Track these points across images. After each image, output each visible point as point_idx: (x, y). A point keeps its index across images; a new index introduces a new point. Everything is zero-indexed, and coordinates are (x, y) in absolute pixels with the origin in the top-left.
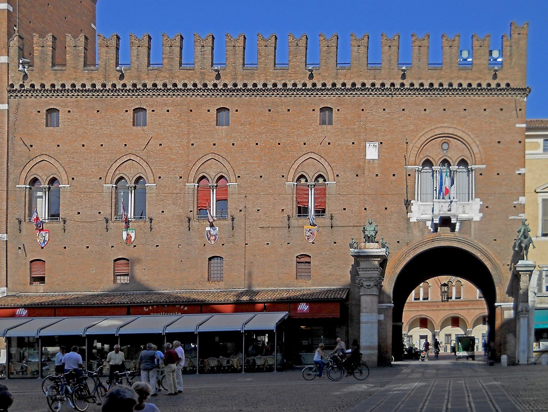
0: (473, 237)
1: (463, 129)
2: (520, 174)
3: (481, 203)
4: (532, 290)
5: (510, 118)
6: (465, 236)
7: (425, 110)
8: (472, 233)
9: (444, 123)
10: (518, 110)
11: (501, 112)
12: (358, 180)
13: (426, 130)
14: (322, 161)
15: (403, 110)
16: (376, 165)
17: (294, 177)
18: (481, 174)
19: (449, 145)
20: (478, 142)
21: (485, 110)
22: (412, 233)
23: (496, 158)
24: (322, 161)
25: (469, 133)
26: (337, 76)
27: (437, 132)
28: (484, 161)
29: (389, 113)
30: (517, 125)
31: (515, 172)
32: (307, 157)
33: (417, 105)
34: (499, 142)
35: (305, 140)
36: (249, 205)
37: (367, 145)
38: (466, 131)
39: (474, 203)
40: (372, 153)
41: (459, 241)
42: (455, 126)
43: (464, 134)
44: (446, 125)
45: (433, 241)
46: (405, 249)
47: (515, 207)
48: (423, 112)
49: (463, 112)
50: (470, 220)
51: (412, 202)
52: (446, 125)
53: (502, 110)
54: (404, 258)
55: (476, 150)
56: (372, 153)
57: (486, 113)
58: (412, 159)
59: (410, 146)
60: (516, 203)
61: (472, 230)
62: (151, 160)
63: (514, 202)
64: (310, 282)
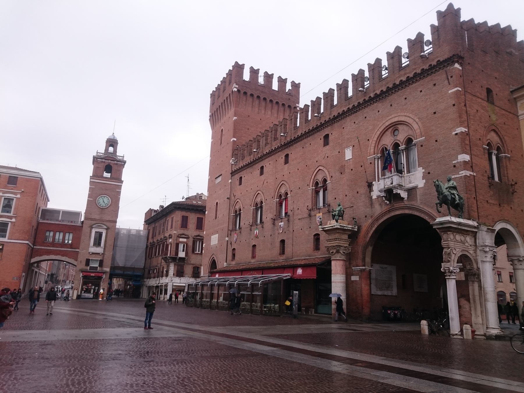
0: (418, 203)
1: (405, 114)
2: (456, 134)
3: (424, 170)
4: (480, 248)
5: (443, 88)
6: (413, 203)
7: (379, 111)
8: (418, 199)
9: (391, 115)
10: (449, 78)
11: (435, 88)
12: (342, 176)
13: (380, 126)
14: (324, 170)
15: (366, 117)
16: (351, 163)
17: (313, 184)
18: (422, 146)
19: (397, 130)
20: (417, 120)
21: (421, 91)
22: (374, 207)
23: (434, 128)
24: (324, 170)
25: (410, 115)
26: (330, 114)
27: (387, 124)
28: (423, 134)
29: (357, 124)
30: (450, 92)
31: (451, 133)
32: (318, 169)
33: (373, 110)
34: (435, 113)
35: (317, 159)
36: (295, 207)
37: (346, 151)
38: (408, 115)
39: (417, 172)
40: (348, 154)
41: (409, 208)
42: (399, 114)
43: (406, 118)
44: (393, 116)
45: (389, 211)
46: (370, 221)
47: (455, 166)
48: (377, 114)
49: (404, 101)
50: (415, 188)
51: (373, 183)
52: (393, 116)
53: (435, 85)
54: (371, 229)
55: (415, 126)
56: (348, 154)
57: (422, 93)
58: (372, 150)
59: (371, 141)
60: (455, 162)
61: (418, 196)
62: (264, 192)
63: (454, 162)
64: (320, 252)
